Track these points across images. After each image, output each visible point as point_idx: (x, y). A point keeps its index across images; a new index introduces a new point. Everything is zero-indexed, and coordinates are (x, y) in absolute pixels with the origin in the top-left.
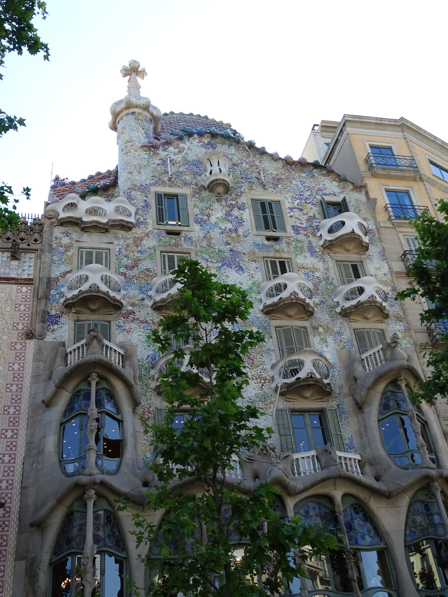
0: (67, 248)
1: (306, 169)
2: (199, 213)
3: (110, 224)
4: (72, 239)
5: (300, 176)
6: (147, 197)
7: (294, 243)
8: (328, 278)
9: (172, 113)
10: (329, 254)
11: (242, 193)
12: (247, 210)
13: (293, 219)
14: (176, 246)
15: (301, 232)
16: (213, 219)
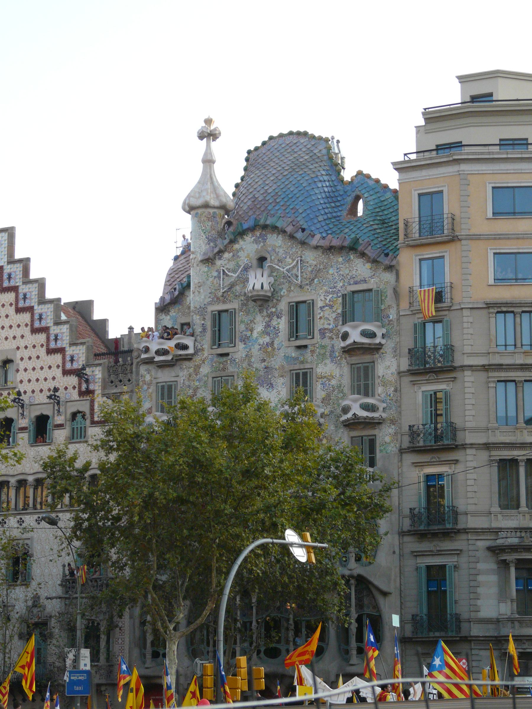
0: (149, 384)
1: (344, 252)
2: (244, 329)
3: (175, 358)
4: (151, 376)
5: (337, 260)
6: (204, 319)
7: (318, 350)
8: (340, 387)
9: (271, 138)
10: (346, 358)
11: (282, 297)
12: (283, 318)
13: (322, 321)
14: (224, 371)
15: (327, 334)
16: (255, 334)
